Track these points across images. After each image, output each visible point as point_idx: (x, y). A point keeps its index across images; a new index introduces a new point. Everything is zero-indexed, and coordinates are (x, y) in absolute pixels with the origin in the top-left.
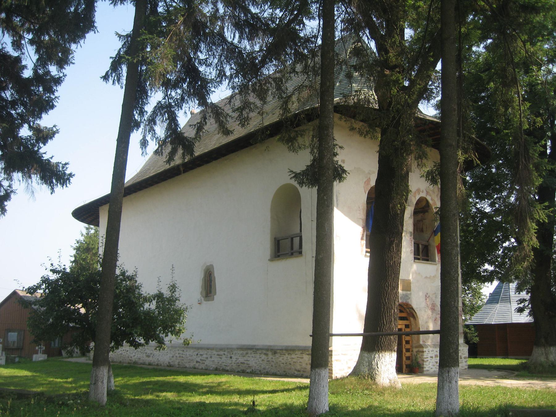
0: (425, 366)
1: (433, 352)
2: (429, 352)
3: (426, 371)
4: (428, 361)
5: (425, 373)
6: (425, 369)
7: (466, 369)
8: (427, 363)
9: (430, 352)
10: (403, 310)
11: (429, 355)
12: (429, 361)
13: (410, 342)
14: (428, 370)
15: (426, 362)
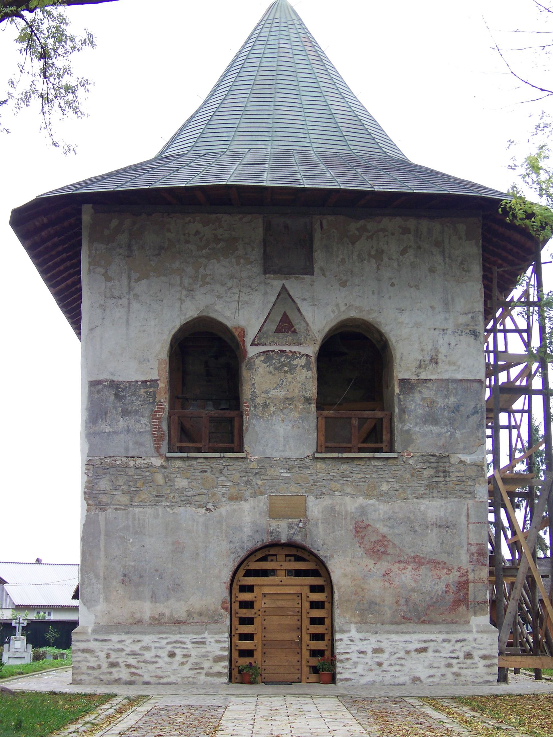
0: (338, 670)
1: (365, 642)
2: (352, 641)
3: (341, 680)
4: (348, 659)
5: (339, 684)
6: (338, 677)
7: (488, 682)
8: (347, 665)
9: (358, 642)
10: (305, 556)
11: (354, 648)
12: (355, 659)
13: (327, 621)
14: (347, 680)
15: (341, 661)
